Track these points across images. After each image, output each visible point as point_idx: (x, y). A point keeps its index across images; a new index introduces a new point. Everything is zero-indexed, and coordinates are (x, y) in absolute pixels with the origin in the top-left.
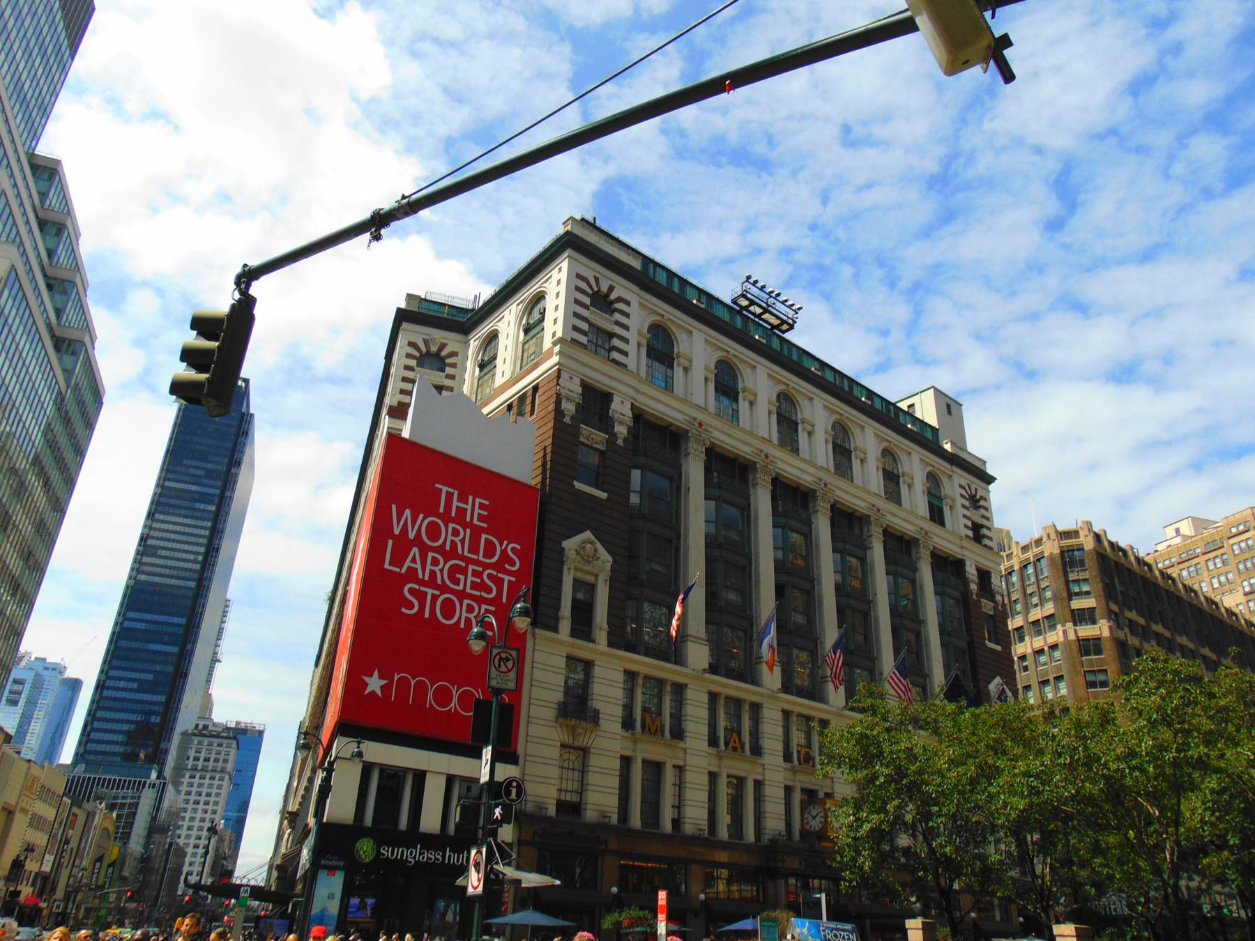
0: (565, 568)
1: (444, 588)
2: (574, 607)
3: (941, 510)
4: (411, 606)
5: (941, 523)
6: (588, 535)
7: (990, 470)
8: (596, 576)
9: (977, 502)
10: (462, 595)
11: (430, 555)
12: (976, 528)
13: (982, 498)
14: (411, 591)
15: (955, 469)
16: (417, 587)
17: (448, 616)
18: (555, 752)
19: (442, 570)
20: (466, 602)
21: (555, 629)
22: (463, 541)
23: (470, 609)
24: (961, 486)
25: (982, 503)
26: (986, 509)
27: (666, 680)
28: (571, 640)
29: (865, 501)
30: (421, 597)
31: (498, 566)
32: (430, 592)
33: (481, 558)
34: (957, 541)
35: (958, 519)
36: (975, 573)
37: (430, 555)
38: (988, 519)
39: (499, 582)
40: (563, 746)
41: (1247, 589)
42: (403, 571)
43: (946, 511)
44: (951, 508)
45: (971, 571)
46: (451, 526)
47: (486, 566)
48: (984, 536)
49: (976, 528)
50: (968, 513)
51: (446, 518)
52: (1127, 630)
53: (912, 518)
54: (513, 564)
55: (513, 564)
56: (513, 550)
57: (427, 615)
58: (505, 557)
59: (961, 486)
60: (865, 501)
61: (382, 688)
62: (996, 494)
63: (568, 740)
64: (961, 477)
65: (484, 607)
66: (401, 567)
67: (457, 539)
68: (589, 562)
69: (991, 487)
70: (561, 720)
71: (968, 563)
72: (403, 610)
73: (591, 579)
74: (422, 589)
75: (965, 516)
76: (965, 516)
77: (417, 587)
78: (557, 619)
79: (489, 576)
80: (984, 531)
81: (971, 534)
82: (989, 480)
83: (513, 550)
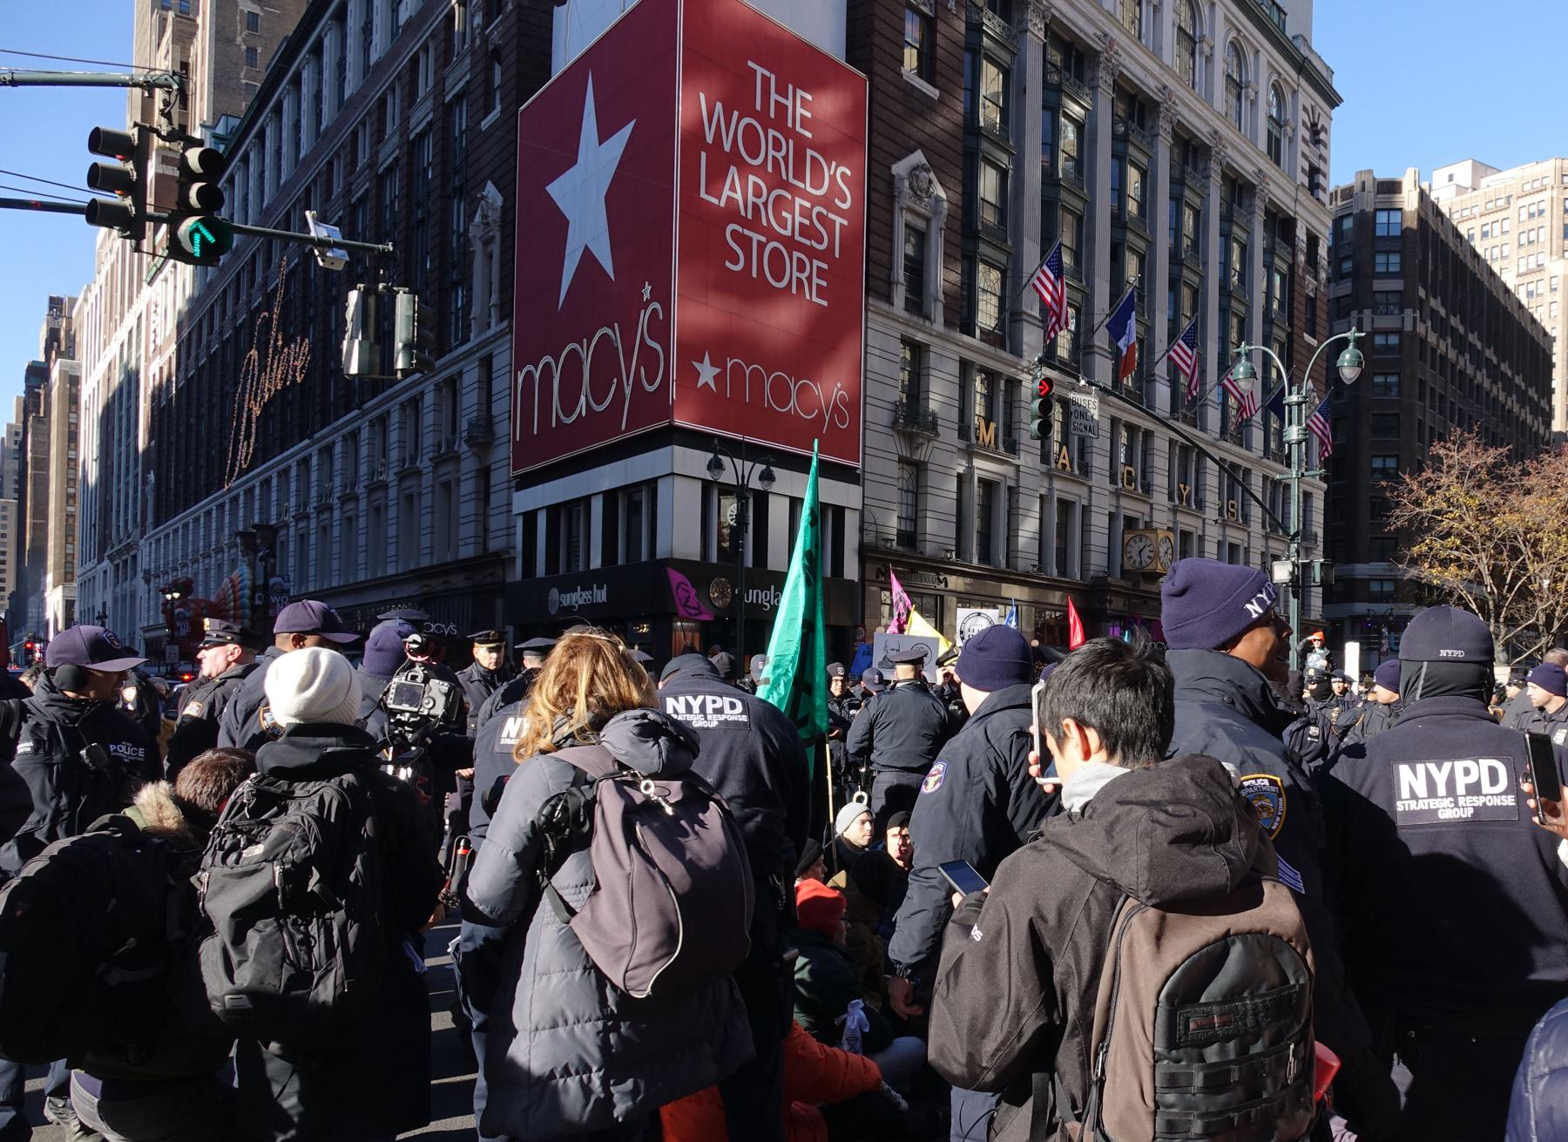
0: (897, 206)
1: (771, 235)
2: (906, 268)
3: (1278, 141)
4: (736, 262)
5: (1278, 162)
6: (918, 157)
7: (1337, 84)
8: (928, 220)
9: (1316, 134)
10: (790, 243)
11: (752, 178)
12: (1314, 172)
13: (1324, 129)
14: (734, 232)
15: (1303, 82)
16: (739, 229)
17: (779, 279)
19: (765, 204)
20: (796, 254)
21: (889, 300)
22: (786, 158)
23: (801, 268)
24: (1305, 109)
25: (1322, 136)
26: (1325, 146)
28: (906, 315)
29: (1207, 123)
30: (745, 242)
31: (826, 202)
32: (756, 237)
33: (809, 189)
34: (1292, 191)
35: (1299, 153)
36: (1305, 238)
37: (752, 178)
38: (1325, 161)
39: (829, 225)
41: (1523, 269)
42: (722, 204)
43: (1284, 143)
44: (1291, 140)
45: (1301, 234)
46: (771, 132)
47: (815, 201)
48: (1318, 186)
49: (1314, 172)
50: (1307, 152)
51: (767, 124)
52: (1429, 323)
53: (1252, 155)
54: (844, 201)
55: (844, 201)
56: (843, 174)
57: (754, 275)
58: (834, 190)
59: (1305, 109)
60: (1207, 123)
62: (1339, 124)
64: (1308, 96)
65: (816, 263)
66: (719, 199)
67: (779, 156)
68: (921, 199)
69: (1335, 112)
71: (1299, 224)
72: (728, 264)
73: (921, 224)
74: (746, 232)
75: (1304, 155)
76: (1304, 155)
77: (739, 229)
78: (890, 283)
79: (819, 215)
80: (1321, 180)
81: (1306, 181)
82: (1333, 100)
83: (843, 174)
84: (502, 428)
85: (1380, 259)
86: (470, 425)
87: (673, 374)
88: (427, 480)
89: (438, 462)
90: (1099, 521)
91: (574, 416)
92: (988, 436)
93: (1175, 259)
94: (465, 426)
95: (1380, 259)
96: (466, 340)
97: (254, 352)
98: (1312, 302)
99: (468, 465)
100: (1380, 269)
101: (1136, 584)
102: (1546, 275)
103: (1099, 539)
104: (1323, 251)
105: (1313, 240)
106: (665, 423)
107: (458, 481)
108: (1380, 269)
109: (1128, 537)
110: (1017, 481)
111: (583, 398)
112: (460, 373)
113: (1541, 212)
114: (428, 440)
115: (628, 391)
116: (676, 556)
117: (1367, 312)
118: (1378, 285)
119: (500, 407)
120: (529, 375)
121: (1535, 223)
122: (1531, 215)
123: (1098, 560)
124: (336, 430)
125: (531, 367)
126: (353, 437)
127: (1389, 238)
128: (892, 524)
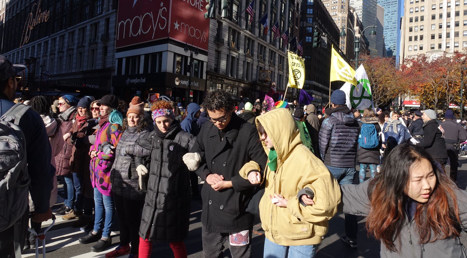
18: (214, 52)
27: (236, 31)
40: (216, 51)
45: (296, 3)
61: (179, 27)
63: (217, 49)
70: (216, 42)
84: (112, 36)
85: (308, 10)
86: (102, 35)
87: (169, 26)
88: (86, 48)
89: (90, 44)
90: (255, 67)
91: (137, 35)
92: (233, 46)
93: (272, 7)
94: (100, 35)
95: (308, 10)
96: (102, 13)
97: (31, 13)
98: (297, 18)
99: (100, 45)
100: (308, 12)
101: (262, 83)
102: (337, 16)
103: (255, 72)
104: (300, 7)
105: (298, 4)
106: (167, 38)
107: (97, 49)
108: (308, 12)
109: (261, 72)
110: (239, 57)
111: (140, 30)
112: (99, 22)
113: (337, 2)
114: (87, 38)
115: (155, 29)
116: (167, 71)
117: (305, 22)
118: (307, 16)
119: (111, 31)
120: (122, 24)
121: (335, 4)
122: (334, 3)
123: (254, 77)
124: (58, 34)
125: (123, 22)
126: (63, 36)
127: (310, 5)
128: (213, 66)
